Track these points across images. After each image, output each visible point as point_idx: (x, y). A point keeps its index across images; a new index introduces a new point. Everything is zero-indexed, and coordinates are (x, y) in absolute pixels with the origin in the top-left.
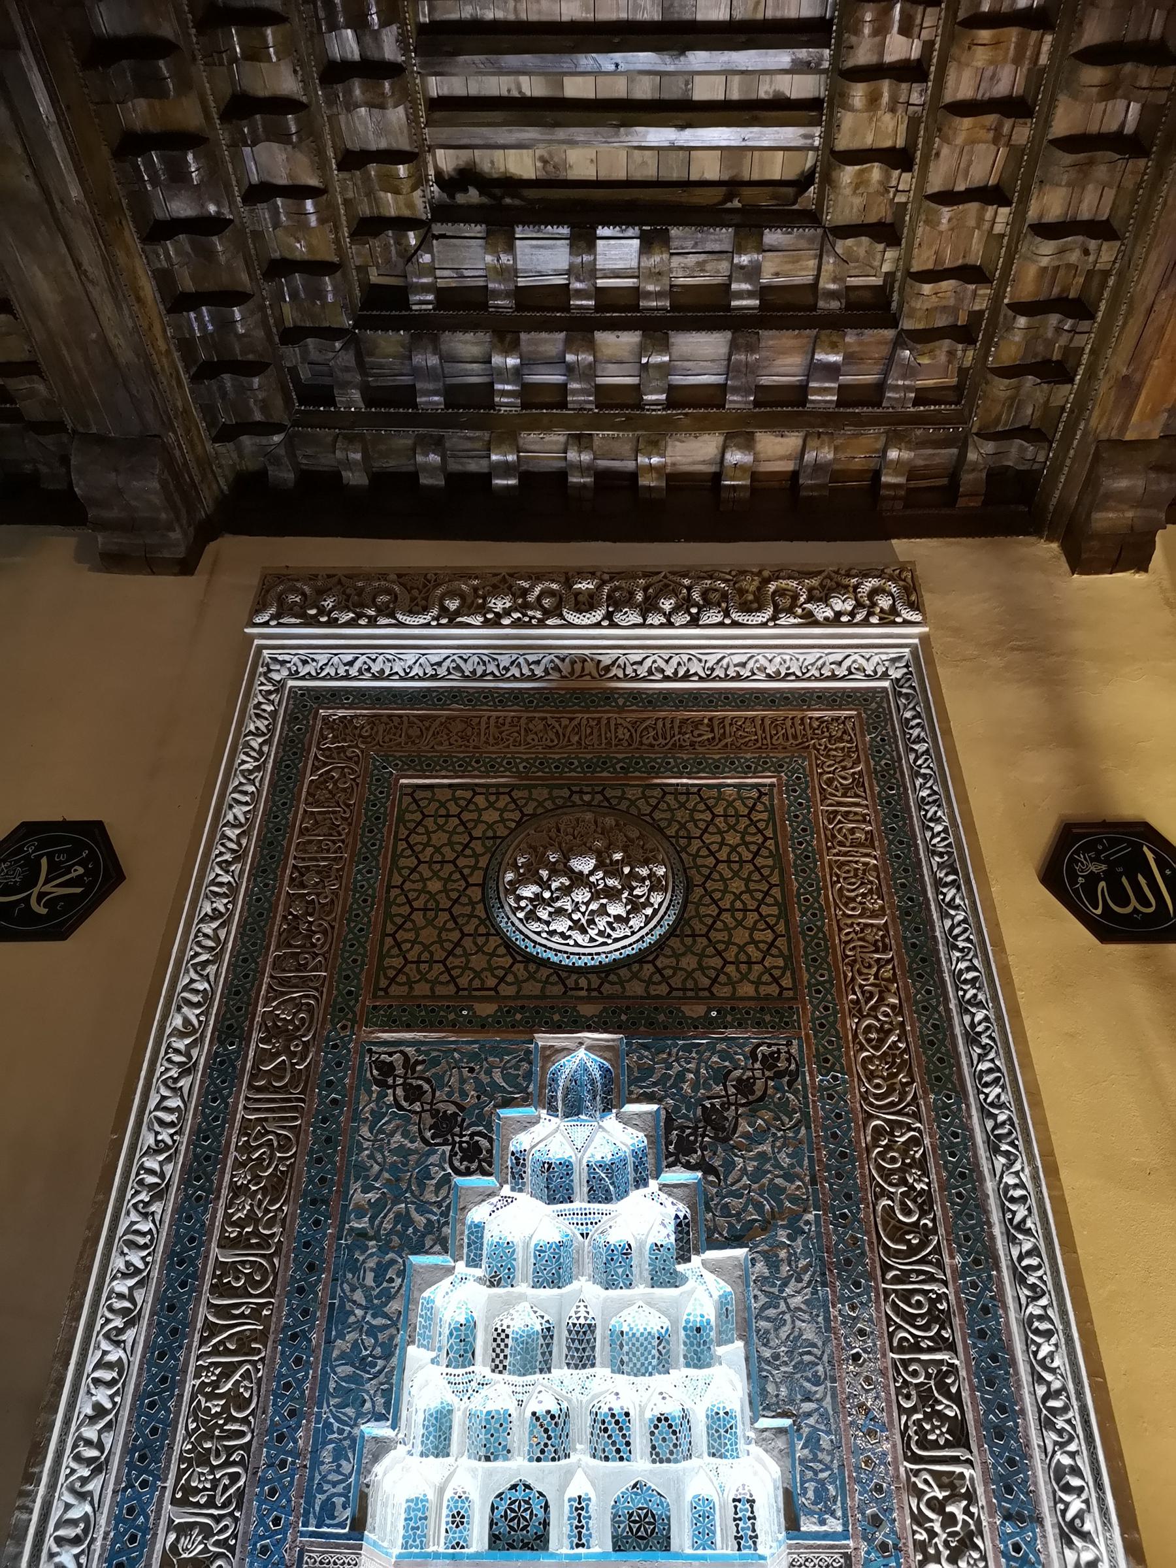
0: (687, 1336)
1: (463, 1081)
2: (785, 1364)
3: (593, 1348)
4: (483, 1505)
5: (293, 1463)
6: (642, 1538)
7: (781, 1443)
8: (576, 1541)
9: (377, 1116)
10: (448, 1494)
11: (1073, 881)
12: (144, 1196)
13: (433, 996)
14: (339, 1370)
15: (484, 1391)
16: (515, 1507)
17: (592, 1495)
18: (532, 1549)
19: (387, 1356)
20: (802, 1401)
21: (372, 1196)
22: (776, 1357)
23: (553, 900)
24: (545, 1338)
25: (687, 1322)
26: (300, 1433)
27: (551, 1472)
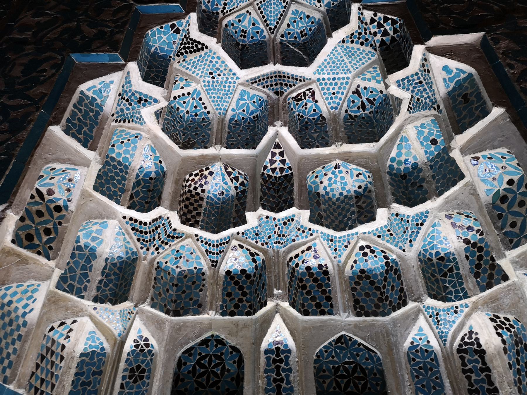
4: (168, 360)
10: (129, 346)
15: (176, 244)
16: (205, 362)
17: (291, 343)
25: (391, 167)
27: (246, 326)
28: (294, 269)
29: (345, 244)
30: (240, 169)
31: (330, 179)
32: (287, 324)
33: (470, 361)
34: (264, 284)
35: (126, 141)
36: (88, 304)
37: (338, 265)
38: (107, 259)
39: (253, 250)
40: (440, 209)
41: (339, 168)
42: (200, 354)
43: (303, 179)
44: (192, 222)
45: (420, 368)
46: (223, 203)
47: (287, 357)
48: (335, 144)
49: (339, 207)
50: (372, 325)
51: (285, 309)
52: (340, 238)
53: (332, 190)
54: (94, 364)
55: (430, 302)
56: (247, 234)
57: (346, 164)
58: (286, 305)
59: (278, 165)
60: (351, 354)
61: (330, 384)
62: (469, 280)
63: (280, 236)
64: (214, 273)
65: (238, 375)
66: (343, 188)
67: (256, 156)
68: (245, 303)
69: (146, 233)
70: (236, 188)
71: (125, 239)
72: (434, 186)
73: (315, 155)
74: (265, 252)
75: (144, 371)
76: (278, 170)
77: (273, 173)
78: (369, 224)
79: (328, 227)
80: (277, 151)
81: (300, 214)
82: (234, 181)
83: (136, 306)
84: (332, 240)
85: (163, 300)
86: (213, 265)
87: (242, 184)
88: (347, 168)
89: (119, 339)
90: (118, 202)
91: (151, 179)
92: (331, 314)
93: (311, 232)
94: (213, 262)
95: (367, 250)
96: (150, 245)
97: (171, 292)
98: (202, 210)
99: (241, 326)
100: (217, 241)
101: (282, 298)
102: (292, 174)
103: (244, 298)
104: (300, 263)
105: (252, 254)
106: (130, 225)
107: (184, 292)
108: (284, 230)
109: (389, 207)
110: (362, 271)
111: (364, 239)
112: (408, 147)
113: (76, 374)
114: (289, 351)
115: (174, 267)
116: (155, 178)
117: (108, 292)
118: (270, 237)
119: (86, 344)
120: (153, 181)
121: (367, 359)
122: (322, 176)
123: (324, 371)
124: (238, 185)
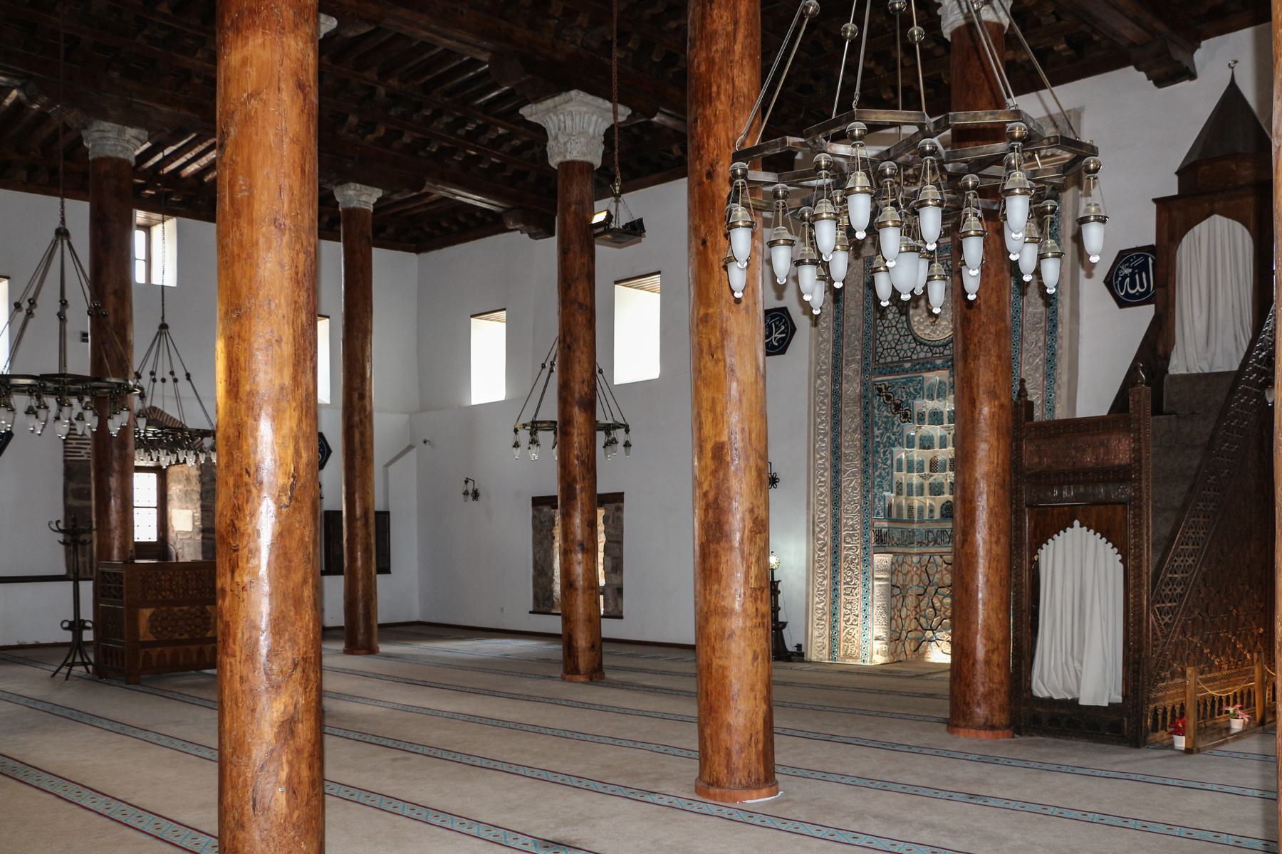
1: (902, 392)
9: (879, 406)
11: (1116, 280)
12: (821, 437)
13: (892, 362)
21: (880, 431)
23: (924, 322)
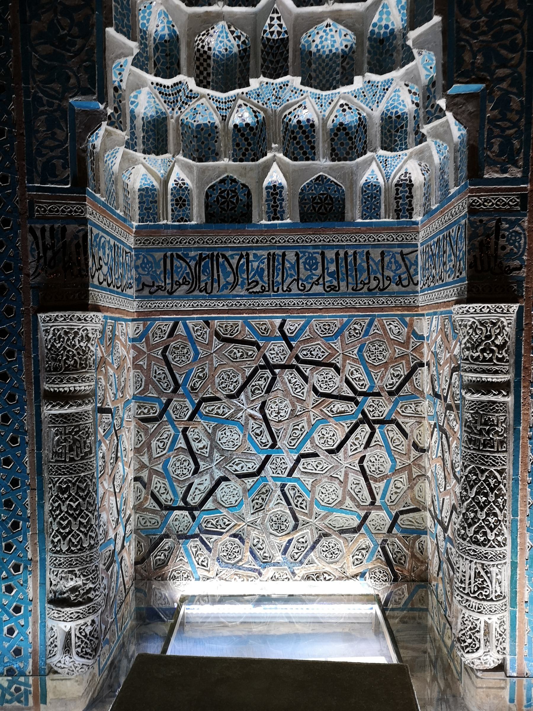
0: (371, 45)
2: (484, 33)
3: (286, 59)
4: (199, 193)
5: (10, 131)
6: (323, 214)
7: (470, 108)
8: (272, 215)
10: (171, 184)
14: (40, 48)
15: (194, 104)
17: (284, 182)
18: (239, 222)
19: (86, 34)
20: (497, 67)
22: (475, 26)
24: (242, 58)
25: (372, 32)
26: (12, 106)
27: (251, 169)
28: (287, 123)
29: (330, 101)
30: (242, 29)
31: (321, 37)
32: (281, 170)
33: (402, 192)
34: (264, 139)
35: (143, 8)
36: (140, 155)
37: (323, 119)
38: (143, 118)
39: (255, 109)
40: (402, 78)
41: (330, 26)
42: (220, 189)
43: (297, 42)
44: (205, 83)
45: (368, 197)
46: (228, 59)
47: (281, 192)
48: (328, 3)
49: (327, 65)
50: (343, 168)
51: (280, 158)
52: (326, 96)
53: (323, 47)
54: (150, 196)
55: (381, 152)
56: (250, 95)
57: (336, 23)
58: (281, 155)
59: (276, 28)
60: (325, 188)
61: (309, 207)
62: (411, 136)
63: (277, 98)
64: (224, 126)
65: (248, 203)
66: (333, 46)
67: (256, 14)
68: (250, 151)
69: (170, 95)
70: (238, 46)
71: (155, 102)
72: (401, 56)
73: (309, 13)
74: (265, 111)
75: (184, 201)
76: (275, 33)
77: (272, 35)
78: (348, 86)
79: (316, 88)
80: (275, 16)
81: (293, 80)
82: (237, 39)
83: (173, 156)
84: (319, 98)
85: (190, 150)
86: (223, 119)
87: (244, 42)
88: (336, 27)
89: (162, 179)
90: (147, 72)
91: (166, 41)
92: (313, 159)
93: (302, 93)
94: (223, 116)
95: (346, 107)
96: (174, 106)
97: (193, 143)
98: (210, 70)
99: (247, 170)
100: (225, 98)
101: (278, 151)
102: (288, 37)
103: (250, 148)
104: (292, 118)
105: (254, 112)
106: (158, 89)
107: (203, 143)
108: (280, 93)
109: (363, 75)
110: (341, 124)
111: (344, 98)
112: (388, 13)
113: (140, 203)
114: (283, 187)
115: (193, 121)
116: (169, 41)
117: (150, 146)
118: (269, 99)
119: (141, 182)
120: (167, 44)
121: (335, 192)
122: (314, 35)
123: (306, 200)
124: (240, 43)
